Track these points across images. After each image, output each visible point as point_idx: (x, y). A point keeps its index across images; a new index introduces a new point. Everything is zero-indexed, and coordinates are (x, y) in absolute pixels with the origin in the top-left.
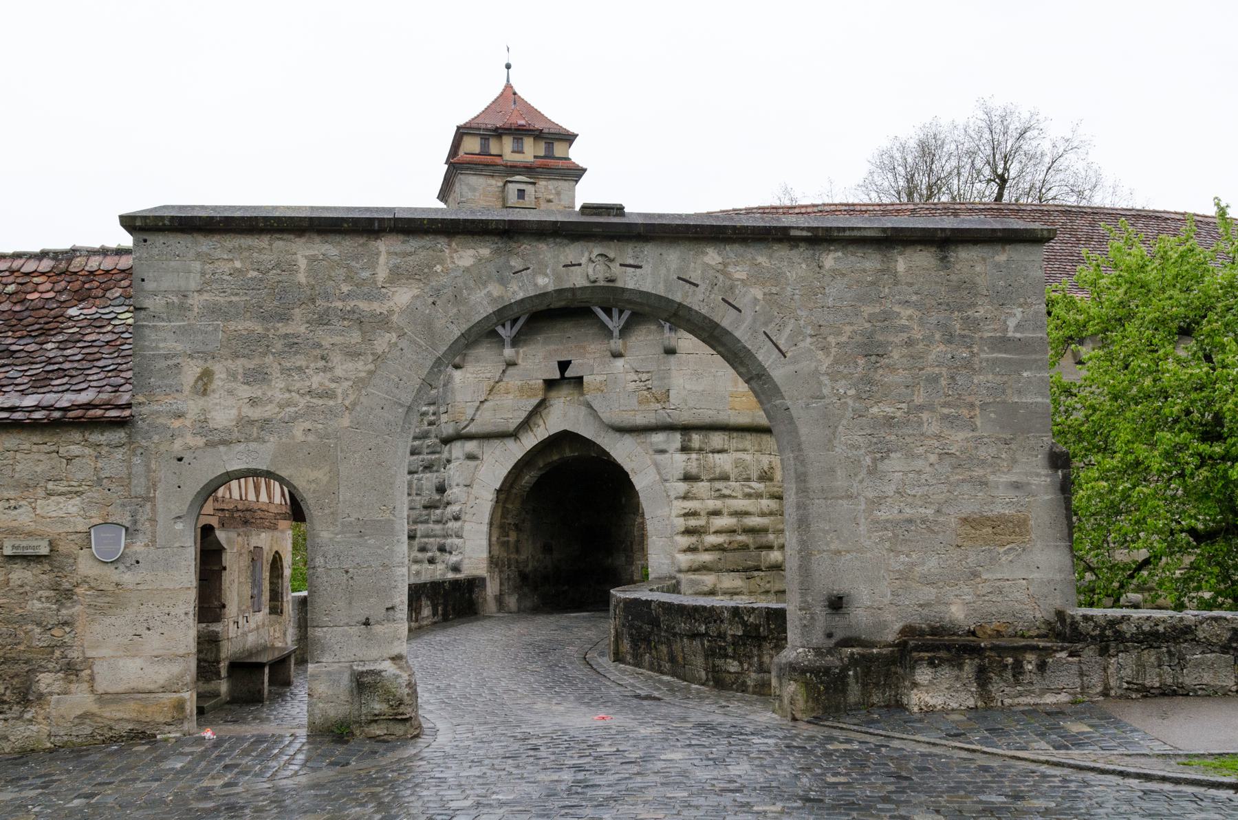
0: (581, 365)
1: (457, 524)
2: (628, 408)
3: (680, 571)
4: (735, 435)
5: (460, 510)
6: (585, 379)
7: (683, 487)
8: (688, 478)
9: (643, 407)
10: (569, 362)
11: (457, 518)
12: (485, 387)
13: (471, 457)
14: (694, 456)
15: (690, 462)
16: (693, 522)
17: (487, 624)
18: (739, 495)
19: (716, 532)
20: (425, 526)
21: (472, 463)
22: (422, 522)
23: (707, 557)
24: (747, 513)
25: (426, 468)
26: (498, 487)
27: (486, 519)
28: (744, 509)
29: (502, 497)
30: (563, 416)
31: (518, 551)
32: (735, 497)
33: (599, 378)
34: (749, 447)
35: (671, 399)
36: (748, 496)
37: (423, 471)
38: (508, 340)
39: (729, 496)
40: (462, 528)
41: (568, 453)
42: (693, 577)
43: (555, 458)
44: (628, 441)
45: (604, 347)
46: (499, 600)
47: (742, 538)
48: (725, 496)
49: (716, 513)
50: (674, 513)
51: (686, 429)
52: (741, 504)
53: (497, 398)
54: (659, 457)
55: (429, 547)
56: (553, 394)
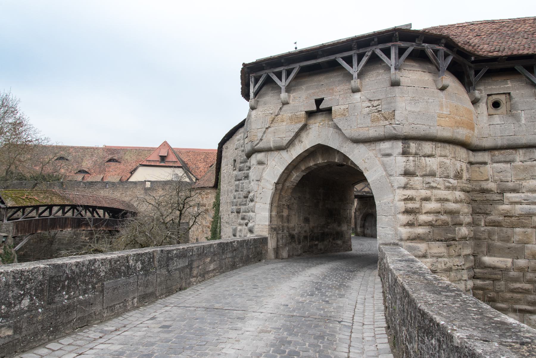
0: (331, 100)
1: (252, 204)
2: (364, 125)
3: (401, 240)
4: (439, 145)
5: (254, 195)
6: (333, 109)
7: (403, 180)
8: (407, 173)
9: (375, 124)
10: (323, 99)
11: (252, 201)
12: (269, 118)
13: (260, 163)
14: (411, 158)
15: (411, 163)
16: (410, 205)
17: (267, 263)
18: (442, 187)
19: (426, 213)
20: (245, 207)
21: (261, 167)
22: (243, 205)
23: (420, 230)
24: (447, 200)
25: (245, 177)
26: (276, 181)
27: (269, 201)
28: (445, 197)
29: (280, 186)
30: (318, 134)
31: (288, 221)
32: (439, 189)
33: (343, 107)
34: (448, 154)
35: (397, 117)
36: (448, 188)
37: (244, 179)
38: (283, 89)
39: (435, 188)
40: (254, 206)
41: (320, 161)
42: (410, 244)
43: (312, 164)
44: (362, 148)
45: (346, 87)
46: (277, 251)
47: (445, 217)
48: (433, 188)
49: (427, 199)
50: (397, 198)
51: (406, 139)
52: (443, 194)
53: (276, 125)
54: (386, 159)
55: (246, 217)
56: (312, 121)
